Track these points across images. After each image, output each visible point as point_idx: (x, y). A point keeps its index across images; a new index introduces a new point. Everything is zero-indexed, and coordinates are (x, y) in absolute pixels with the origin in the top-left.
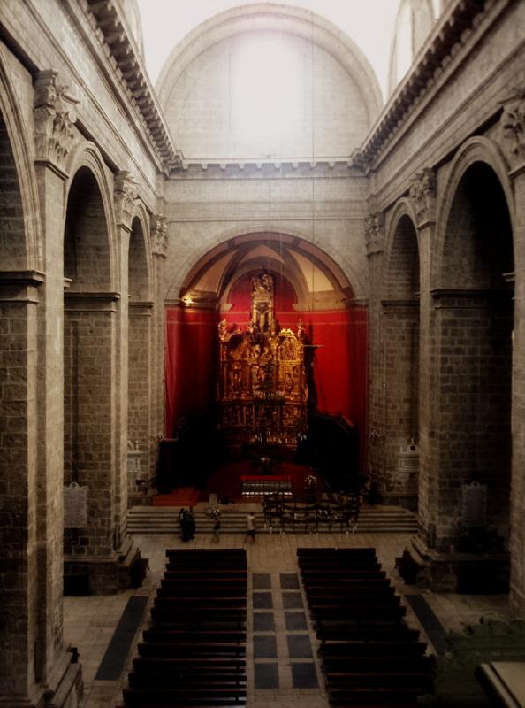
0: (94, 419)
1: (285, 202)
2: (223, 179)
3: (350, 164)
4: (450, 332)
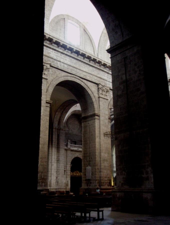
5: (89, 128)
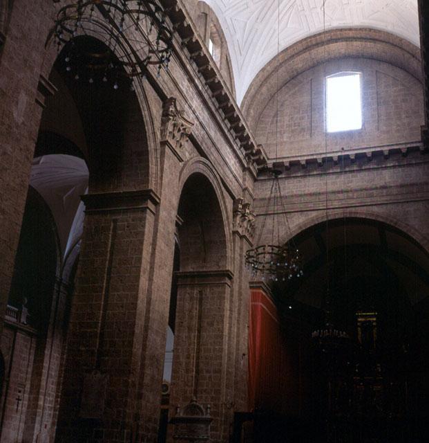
0: (122, 307)
1: (361, 190)
3: (422, 148)
5: (114, 236)
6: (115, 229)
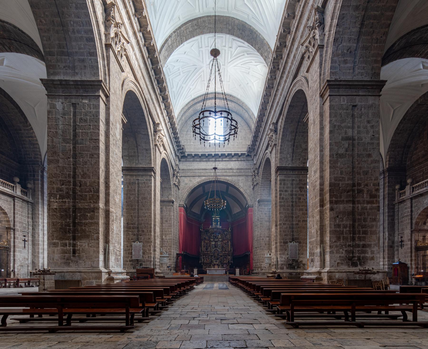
2: (200, 161)
4: (283, 184)
5: (139, 187)
6: (138, 184)
